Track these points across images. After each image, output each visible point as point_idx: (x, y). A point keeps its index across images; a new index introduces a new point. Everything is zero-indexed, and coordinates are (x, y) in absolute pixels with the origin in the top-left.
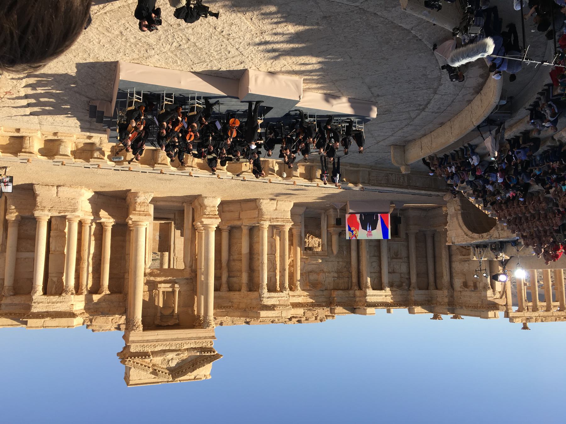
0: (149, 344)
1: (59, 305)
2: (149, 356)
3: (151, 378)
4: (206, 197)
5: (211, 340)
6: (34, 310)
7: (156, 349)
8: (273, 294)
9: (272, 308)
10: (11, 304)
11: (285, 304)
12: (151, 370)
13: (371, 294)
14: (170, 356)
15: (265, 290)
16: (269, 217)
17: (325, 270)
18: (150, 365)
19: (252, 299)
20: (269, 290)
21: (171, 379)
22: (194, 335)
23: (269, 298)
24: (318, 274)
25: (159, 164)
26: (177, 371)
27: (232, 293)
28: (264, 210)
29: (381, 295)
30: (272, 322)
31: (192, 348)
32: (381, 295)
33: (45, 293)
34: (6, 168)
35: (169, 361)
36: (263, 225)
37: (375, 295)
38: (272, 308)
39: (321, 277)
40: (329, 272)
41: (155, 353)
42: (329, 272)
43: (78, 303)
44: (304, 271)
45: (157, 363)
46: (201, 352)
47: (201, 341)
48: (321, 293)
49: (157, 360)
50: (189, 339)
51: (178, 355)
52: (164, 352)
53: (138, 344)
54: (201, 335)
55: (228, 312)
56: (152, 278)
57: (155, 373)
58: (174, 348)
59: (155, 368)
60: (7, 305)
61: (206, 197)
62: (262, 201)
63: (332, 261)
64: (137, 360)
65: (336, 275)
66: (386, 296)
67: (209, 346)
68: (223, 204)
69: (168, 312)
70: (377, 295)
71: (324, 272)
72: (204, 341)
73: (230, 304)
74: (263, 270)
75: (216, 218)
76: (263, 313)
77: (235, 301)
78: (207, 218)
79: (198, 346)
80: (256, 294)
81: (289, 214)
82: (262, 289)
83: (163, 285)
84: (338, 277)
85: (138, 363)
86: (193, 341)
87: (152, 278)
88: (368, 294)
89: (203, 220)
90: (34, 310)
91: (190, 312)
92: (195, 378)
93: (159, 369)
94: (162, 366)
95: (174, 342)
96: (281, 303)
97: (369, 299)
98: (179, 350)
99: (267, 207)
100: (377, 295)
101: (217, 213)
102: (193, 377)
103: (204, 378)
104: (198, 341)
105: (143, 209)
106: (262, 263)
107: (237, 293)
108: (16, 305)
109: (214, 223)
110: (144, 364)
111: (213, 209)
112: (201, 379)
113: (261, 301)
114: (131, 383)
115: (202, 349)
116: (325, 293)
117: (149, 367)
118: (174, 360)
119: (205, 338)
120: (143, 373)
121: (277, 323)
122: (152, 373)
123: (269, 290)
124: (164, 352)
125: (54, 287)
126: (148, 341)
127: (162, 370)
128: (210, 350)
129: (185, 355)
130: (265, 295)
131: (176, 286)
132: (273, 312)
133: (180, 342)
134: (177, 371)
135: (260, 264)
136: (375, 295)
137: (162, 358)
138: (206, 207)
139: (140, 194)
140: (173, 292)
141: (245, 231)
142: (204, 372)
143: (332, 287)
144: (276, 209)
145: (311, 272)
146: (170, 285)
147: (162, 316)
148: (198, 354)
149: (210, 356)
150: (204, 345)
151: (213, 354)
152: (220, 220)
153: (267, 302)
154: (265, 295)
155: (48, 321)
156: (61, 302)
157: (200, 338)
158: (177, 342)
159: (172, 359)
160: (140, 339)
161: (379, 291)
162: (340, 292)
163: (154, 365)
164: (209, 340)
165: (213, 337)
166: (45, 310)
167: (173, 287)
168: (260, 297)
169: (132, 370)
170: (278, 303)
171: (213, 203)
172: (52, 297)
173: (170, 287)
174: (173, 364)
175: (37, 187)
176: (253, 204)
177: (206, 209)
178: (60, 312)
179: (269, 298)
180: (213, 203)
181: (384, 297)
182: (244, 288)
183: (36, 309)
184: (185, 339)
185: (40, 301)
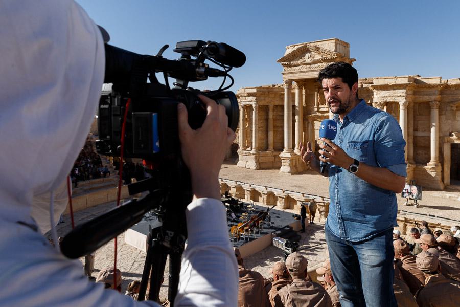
1: (386, 95)
4: (288, 172)
5: (285, 72)
7: (319, 64)
8: (249, 103)
9: (250, 95)
10: (430, 95)
15: (254, 106)
16: (251, 156)
19: (264, 100)
22: (295, 75)
23: (251, 101)
25: (283, 198)
26: (304, 50)
28: (254, 161)
31: (296, 66)
34: (407, 205)
35: (310, 57)
38: (250, 95)
45: (318, 55)
46: (290, 64)
49: (318, 57)
50: (297, 72)
52: (314, 63)
54: (291, 75)
57: (318, 49)
58: (308, 66)
60: (434, 94)
61: (288, 172)
62: (255, 168)
64: (329, 57)
67: (286, 68)
68: (279, 168)
72: (289, 71)
74: (255, 120)
75: (282, 157)
76: (255, 91)
78: (287, 158)
80: (261, 103)
81: (240, 158)
82: (255, 107)
85: (329, 54)
86: (296, 71)
89: (290, 156)
90: (404, 91)
91: (308, 91)
92: (294, 46)
94: (314, 53)
95: (308, 70)
98: (304, 64)
99: (252, 164)
101: (282, 161)
103: (289, 46)
104: (293, 71)
106: (256, 124)
107: (277, 104)
108: (427, 95)
109: (285, 154)
111: (285, 164)
113: (256, 99)
114: (334, 41)
115: (290, 66)
118: (307, 58)
119: (288, 73)
120: (326, 48)
122: (319, 48)
123: (251, 106)
128: (285, 65)
129: (300, 61)
132: (249, 92)
133: (304, 70)
134: (304, 50)
135: (257, 123)
138: (289, 165)
140: (318, 105)
141: (271, 147)
142: (289, 51)
144: (247, 161)
146: (321, 110)
148: (292, 63)
152: (280, 155)
153: (252, 98)
155: (391, 82)
156: (385, 97)
157: (291, 73)
158: (306, 70)
159: (308, 58)
163: (320, 54)
165: (284, 74)
166: (396, 91)
167: (319, 109)
168: (257, 101)
169: (333, 50)
170: (247, 98)
171: (285, 168)
172: (391, 101)
173: (320, 108)
174: (308, 55)
176: (261, 166)
177: (289, 165)
178: (384, 90)
179: (251, 101)
180: (285, 168)
182: (271, 107)
183: (402, 92)
185: (400, 97)
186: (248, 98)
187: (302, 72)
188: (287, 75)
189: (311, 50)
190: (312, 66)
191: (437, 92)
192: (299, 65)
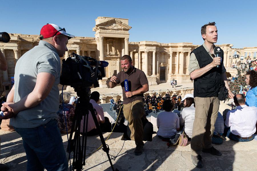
1: (149, 48)
2: (123, 29)
3: (123, 21)
6: (155, 47)
7: (120, 31)
8: (74, 49)
12: (122, 24)
13: (14, 47)
14: (115, 28)
18: (122, 25)
21: (115, 19)
26: (113, 22)
27: (87, 50)
29: (7, 46)
30: (29, 36)
32: (7, 46)
33: (152, 52)
37: (12, 47)
41: (121, 30)
43: (141, 49)
47: (105, 32)
49: (120, 27)
55: (88, 42)
56: (117, 57)
57: (121, 23)
58: (114, 31)
59: (121, 24)
66: (3, 46)
67: (101, 30)
69: (111, 44)
70: (10, 46)
72: (103, 32)
73: (87, 46)
76: (79, 41)
77: (85, 47)
78: (106, 80)
83: (113, 54)
85: (127, 27)
86: (107, 32)
87: (117, 57)
88: (17, 48)
90: (155, 47)
97: (16, 45)
98: (112, 30)
100: (10, 46)
102: (106, 18)
103: (102, 17)
117: (123, 25)
119: (103, 33)
121: (27, 35)
124: (118, 30)
125: (150, 54)
126: (123, 34)
128: (101, 28)
129: (110, 27)
130: (78, 49)
131: (108, 54)
134: (113, 22)
136: (12, 47)
137: (118, 27)
140: (109, 52)
147: (112, 42)
148: (106, 27)
149: (101, 26)
150: (103, 30)
151: (101, 27)
153: (77, 46)
154: (78, 49)
157: (105, 33)
161: (8, 49)
163: (121, 25)
164: (101, 32)
166: (153, 47)
167: (110, 53)
174: (114, 25)
175: (157, 84)
181: (5, 45)
183: (154, 48)
185: (154, 50)
186: (73, 45)
187: (112, 33)
188: (102, 34)
191: (159, 48)
192: (110, 29)
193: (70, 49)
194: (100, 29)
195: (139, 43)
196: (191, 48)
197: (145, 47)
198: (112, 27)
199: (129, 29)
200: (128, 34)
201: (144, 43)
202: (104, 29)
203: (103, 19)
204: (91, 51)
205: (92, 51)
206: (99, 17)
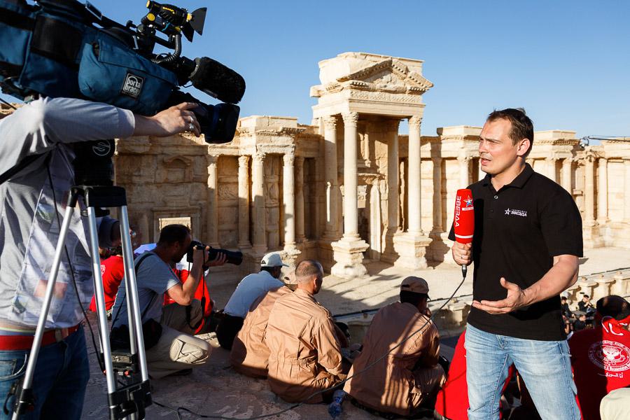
0: (407, 102)
8: (279, 151)
11: (262, 136)
12: (409, 75)
14: (391, 87)
17: (154, 187)
20: (281, 156)
22: (369, 106)
24: (167, 182)
26: (386, 68)
36: (296, 248)
38: (288, 132)
39: (162, 174)
40: (147, 183)
42: (147, 183)
44: (190, 185)
48: (166, 150)
49: (400, 84)
51: (385, 86)
53: (416, 103)
58: (387, 94)
59: (404, 76)
63: (142, 203)
65: (136, 179)
67: (354, 91)
71: (155, 183)
79: (365, 93)
84: (130, 176)
86: (369, 99)
93: (401, 74)
96: (268, 138)
102: (368, 58)
105: (420, 249)
110: (413, 82)
112: (361, 54)
115: (362, 88)
116: (159, 150)
119: (359, 101)
123: (281, 156)
124: (395, 92)
126: (410, 105)
127: (398, 72)
129: (378, 84)
134: (386, 68)
139: (426, 265)
143: (144, 159)
145: (177, 184)
148: (367, 84)
149: (356, 78)
151: (355, 81)
160: (415, 109)
162: (140, 150)
170: (273, 137)
174: (386, 78)
184: (378, 104)
187: (381, 103)
189: (394, 69)
190: (392, 95)
193: (269, 152)
194: (352, 88)
195: (440, 131)
196: (572, 148)
197: (461, 143)
198: (383, 85)
199: (424, 91)
200: (422, 106)
201: (461, 131)
202: (362, 90)
203: (358, 61)
204: (305, 156)
205: (308, 156)
206: (346, 54)
